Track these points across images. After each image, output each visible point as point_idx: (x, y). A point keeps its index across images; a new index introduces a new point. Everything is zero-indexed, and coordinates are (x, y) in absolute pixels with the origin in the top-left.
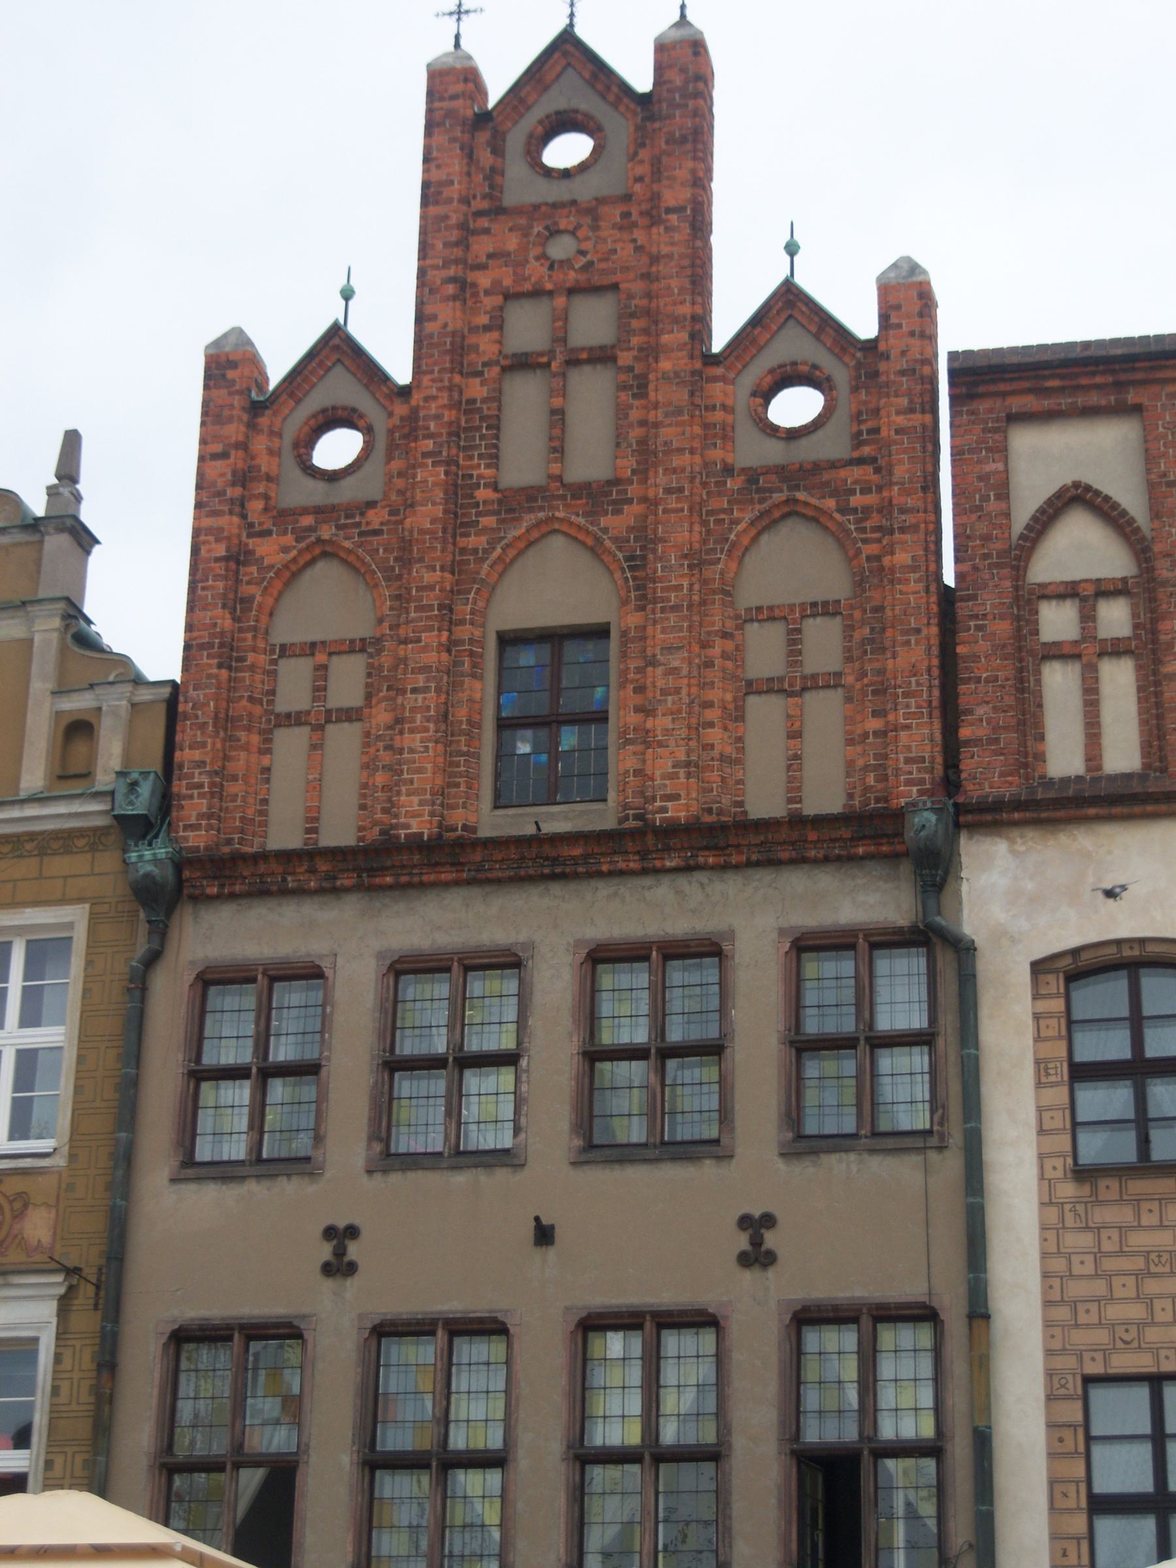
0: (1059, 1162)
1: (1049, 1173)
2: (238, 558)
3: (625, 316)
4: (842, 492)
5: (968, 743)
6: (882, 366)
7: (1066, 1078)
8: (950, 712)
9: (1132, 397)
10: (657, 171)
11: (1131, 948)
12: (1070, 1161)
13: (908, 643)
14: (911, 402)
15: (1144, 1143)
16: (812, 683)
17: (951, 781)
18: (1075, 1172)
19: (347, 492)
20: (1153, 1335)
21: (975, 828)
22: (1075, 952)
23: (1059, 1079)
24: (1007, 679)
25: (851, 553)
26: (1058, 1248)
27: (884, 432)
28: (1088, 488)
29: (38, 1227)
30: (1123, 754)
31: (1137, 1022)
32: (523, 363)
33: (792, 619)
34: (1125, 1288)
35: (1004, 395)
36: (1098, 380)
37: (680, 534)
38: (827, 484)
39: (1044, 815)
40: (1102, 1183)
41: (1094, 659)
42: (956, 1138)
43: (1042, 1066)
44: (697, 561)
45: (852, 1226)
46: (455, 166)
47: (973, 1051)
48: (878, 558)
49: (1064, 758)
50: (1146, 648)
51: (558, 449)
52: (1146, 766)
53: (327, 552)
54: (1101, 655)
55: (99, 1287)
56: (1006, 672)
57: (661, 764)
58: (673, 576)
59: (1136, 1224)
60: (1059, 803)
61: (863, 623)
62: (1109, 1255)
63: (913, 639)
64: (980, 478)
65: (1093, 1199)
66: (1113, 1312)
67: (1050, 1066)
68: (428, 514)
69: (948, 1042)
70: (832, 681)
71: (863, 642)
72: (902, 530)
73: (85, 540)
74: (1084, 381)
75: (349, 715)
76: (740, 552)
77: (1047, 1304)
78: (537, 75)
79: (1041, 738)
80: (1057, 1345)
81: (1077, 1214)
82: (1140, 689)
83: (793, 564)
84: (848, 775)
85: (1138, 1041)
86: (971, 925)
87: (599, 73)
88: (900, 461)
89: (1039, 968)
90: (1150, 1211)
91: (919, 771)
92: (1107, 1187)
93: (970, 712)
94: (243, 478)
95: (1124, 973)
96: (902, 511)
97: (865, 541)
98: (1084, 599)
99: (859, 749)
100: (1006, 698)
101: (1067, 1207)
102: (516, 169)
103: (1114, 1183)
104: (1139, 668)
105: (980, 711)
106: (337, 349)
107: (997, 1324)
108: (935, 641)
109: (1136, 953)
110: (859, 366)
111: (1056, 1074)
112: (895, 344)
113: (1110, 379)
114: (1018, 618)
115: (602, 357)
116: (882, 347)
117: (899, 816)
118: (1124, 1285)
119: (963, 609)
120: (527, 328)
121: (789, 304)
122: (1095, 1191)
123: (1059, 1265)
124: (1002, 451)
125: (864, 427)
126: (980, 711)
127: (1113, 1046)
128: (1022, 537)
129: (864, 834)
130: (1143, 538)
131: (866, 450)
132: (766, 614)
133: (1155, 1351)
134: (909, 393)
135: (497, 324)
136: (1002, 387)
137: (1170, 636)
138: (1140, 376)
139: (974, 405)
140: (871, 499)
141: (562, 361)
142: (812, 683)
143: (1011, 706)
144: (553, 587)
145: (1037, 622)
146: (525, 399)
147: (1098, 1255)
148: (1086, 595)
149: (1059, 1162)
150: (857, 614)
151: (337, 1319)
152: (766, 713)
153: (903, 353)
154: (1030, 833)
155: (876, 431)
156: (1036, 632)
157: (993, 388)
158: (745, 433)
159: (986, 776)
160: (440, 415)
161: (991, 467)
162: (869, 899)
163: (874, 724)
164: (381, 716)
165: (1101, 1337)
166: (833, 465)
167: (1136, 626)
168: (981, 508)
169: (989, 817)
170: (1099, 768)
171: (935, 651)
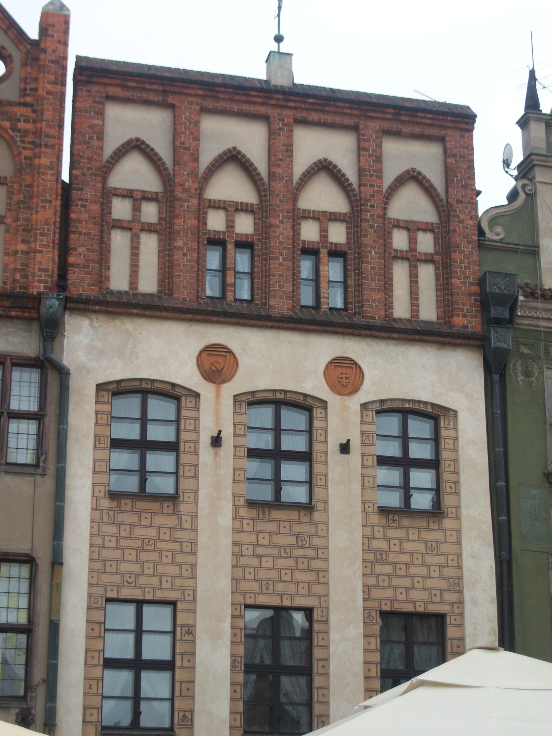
0: (102, 489)
1: (97, 494)
4: (14, 120)
5: (72, 265)
6: (42, 56)
7: (109, 446)
8: (64, 248)
9: (170, 99)
11: (147, 384)
12: (107, 488)
13: (44, 207)
14: (56, 78)
15: (143, 482)
18: (110, 494)
20: (142, 580)
21: (73, 310)
22: (119, 382)
23: (106, 446)
24: (96, 235)
25: (16, 153)
26: (99, 533)
27: (40, 92)
28: (143, 142)
30: (148, 284)
31: (144, 421)
34: (131, 555)
35: (106, 85)
36: (155, 87)
38: (6, 113)
39: (110, 309)
40: (123, 501)
41: (138, 232)
42: (51, 471)
43: (97, 438)
47: (65, 427)
48: (30, 159)
49: (119, 281)
50: (165, 230)
52: (159, 291)
54: (142, 230)
56: (95, 232)
59: (139, 524)
60: (118, 304)
61: (20, 192)
62: (124, 538)
63: (47, 205)
64: (90, 127)
65: (118, 509)
66: (124, 567)
67: (102, 439)
69: (50, 421)
71: (19, 202)
72: (46, 146)
74: (148, 86)
77: (91, 560)
79: (108, 268)
80: (94, 581)
81: (109, 516)
82: (160, 251)
84: (4, 271)
85: (144, 431)
88: (48, 109)
89: (100, 387)
90: (146, 518)
91: (45, 275)
92: (126, 504)
93: (75, 249)
95: (140, 395)
96: (47, 136)
97: (24, 148)
98: (135, 200)
99: (12, 259)
100: (94, 245)
101: (105, 512)
103: (129, 502)
104: (160, 240)
105: (81, 250)
107: (65, 568)
108: (59, 209)
109: (149, 386)
110: (28, 52)
111: (104, 443)
112: (49, 44)
113: (161, 88)
114: (102, 204)
116: (43, 45)
117: (38, 299)
118: (130, 554)
119: (75, 194)
122: (119, 506)
123: (98, 541)
124: (101, 114)
125: (28, 87)
126: (81, 250)
127: (132, 432)
128: (108, 161)
130: (169, 174)
131: (28, 99)
133: (143, 588)
134: (55, 73)
136: (106, 81)
137: (179, 227)
138: (176, 89)
139: (90, 87)
140: (29, 126)
143: (96, 250)
145: (111, 207)
147: (118, 538)
149: (102, 489)
150: (16, 186)
153: (54, 51)
154: (102, 317)
155: (35, 90)
156: (110, 213)
157: (101, 80)
159: (80, 284)
161: (96, 122)
163: (21, 247)
165: (117, 579)
166: (10, 104)
167: (160, 219)
168: (88, 143)
169: (82, 306)
170: (136, 289)
171: (59, 214)
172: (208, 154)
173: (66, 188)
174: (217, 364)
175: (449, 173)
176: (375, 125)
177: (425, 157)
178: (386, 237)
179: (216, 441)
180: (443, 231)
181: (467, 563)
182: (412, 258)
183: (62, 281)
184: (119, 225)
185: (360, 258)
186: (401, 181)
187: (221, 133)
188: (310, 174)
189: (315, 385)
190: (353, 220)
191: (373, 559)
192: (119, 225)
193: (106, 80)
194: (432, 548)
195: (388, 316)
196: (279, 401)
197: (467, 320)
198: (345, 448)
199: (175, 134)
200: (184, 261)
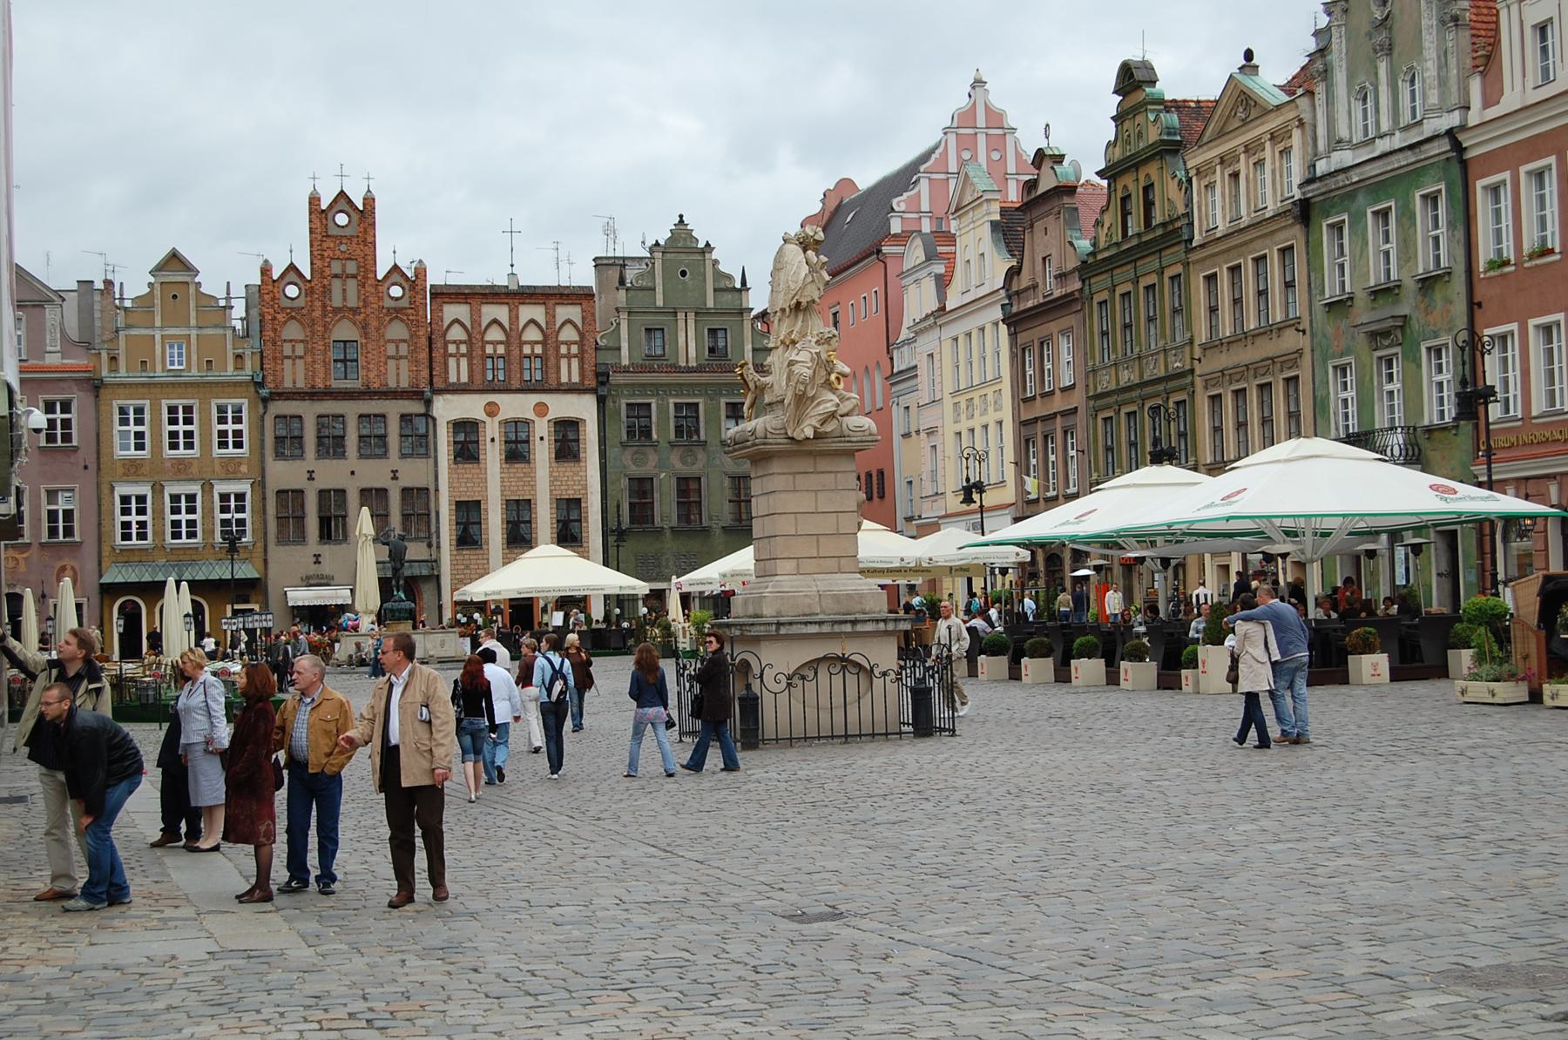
2: (274, 319)
8: (431, 369)
17: (431, 383)
29: (244, 469)
30: (464, 378)
32: (336, 276)
33: (397, 342)
37: (374, 323)
44: (378, 329)
45: (414, 473)
49: (453, 379)
50: (469, 356)
51: (345, 299)
55: (260, 485)
57: (372, 375)
68: (317, 314)
78: (335, 200)
83: (397, 330)
86: (435, 414)
87: (350, 202)
102: (331, 224)
115: (354, 276)
120: (336, 267)
121: (396, 267)
129: (414, 394)
144: (345, 330)
146: (337, 283)
148: (457, 343)
152: (391, 363)
158: (386, 299)
159: (438, 383)
174: (492, 410)
177: (574, 312)
178: (557, 349)
180: (581, 344)
186: (563, 324)
187: (491, 311)
188: (525, 326)
189: (530, 415)
190: (544, 343)
193: (445, 294)
194: (576, 474)
195: (559, 384)
196: (516, 422)
197: (591, 382)
200: (477, 369)
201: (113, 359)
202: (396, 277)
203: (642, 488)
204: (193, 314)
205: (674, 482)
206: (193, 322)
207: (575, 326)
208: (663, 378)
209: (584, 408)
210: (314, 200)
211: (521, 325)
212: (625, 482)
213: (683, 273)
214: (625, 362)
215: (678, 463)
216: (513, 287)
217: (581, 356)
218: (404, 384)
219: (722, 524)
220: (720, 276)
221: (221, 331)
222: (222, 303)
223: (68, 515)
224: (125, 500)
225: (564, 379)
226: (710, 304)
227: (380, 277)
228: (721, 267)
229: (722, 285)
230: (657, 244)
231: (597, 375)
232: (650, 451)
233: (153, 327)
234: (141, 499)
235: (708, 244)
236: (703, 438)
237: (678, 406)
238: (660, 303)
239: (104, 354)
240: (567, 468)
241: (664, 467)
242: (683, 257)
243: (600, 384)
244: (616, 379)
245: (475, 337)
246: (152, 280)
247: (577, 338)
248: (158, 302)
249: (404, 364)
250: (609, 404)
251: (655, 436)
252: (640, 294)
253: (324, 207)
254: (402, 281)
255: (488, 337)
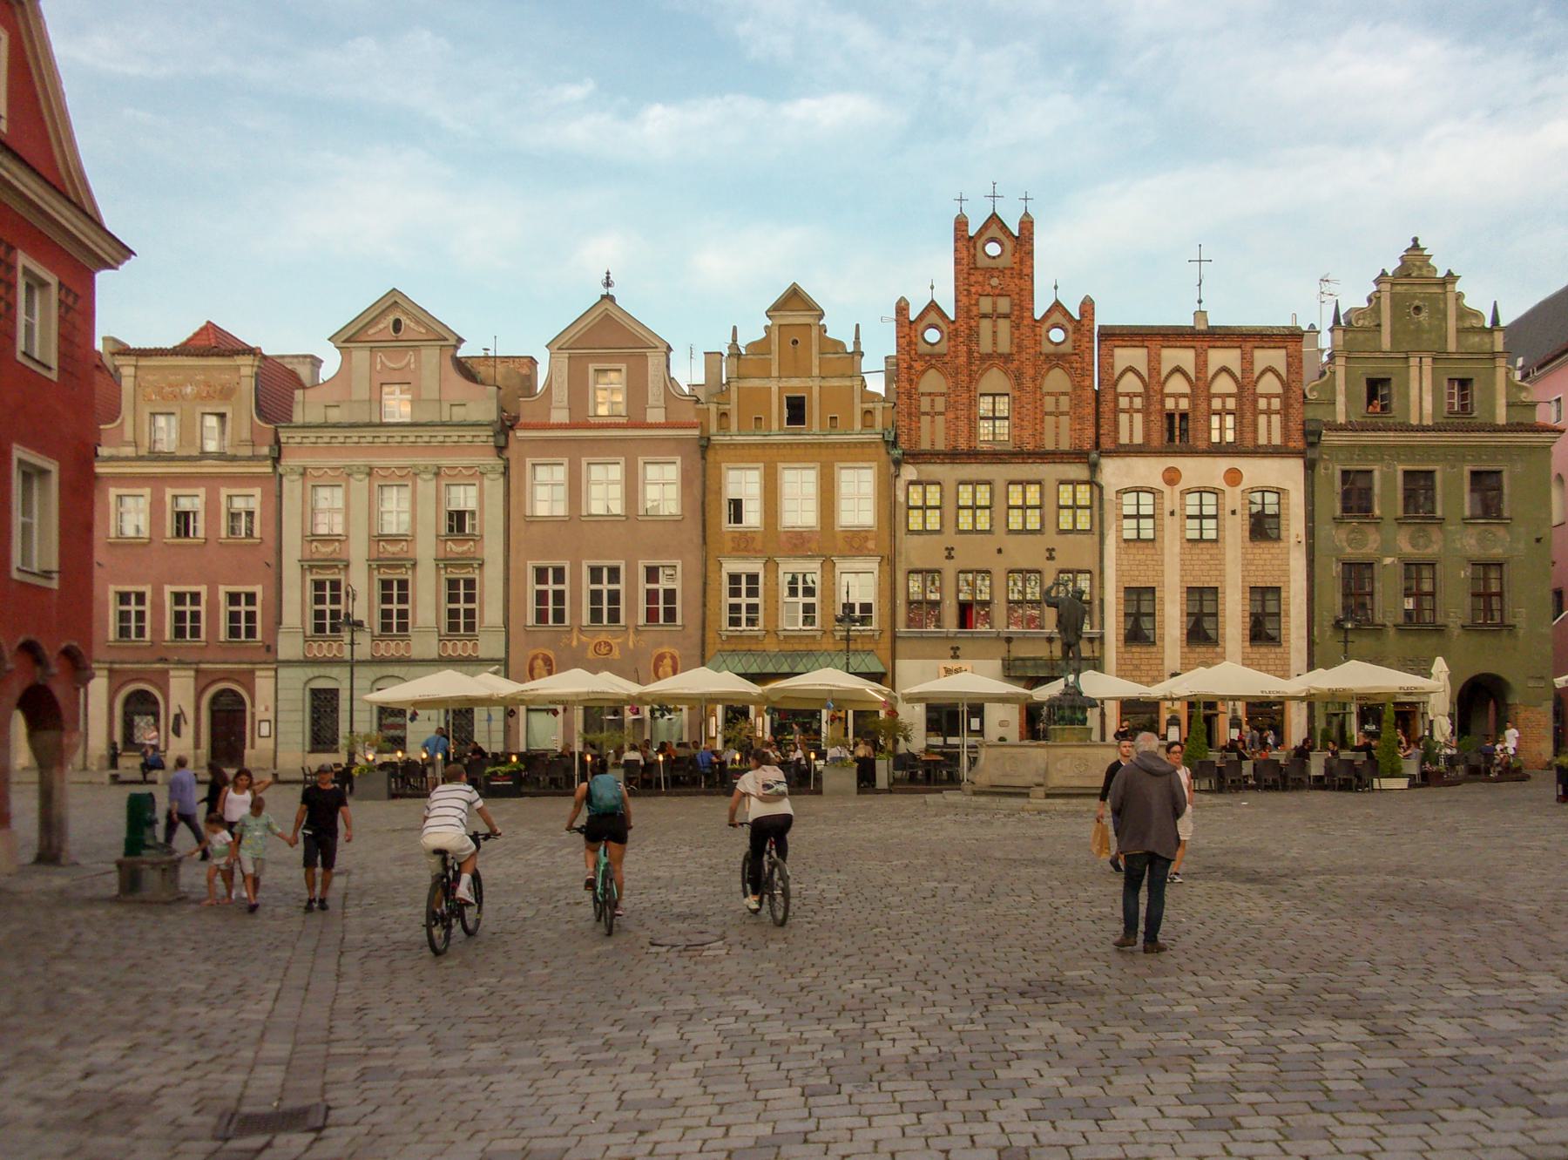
2: (910, 367)
3: (1012, 305)
8: (1098, 426)
10: (1021, 262)
16: (1062, 414)
19: (937, 349)
29: (871, 545)
32: (985, 316)
42: (1097, 532)
44: (1034, 380)
46: (965, 254)
50: (1146, 412)
51: (995, 343)
53: (932, 366)
58: (1028, 384)
68: (962, 360)
69: (1096, 508)
70: (1067, 414)
73: (862, 355)
75: (941, 414)
76: (1043, 377)
78: (985, 226)
83: (1057, 380)
87: (1003, 227)
94: (910, 343)
102: (980, 254)
106: (933, 306)
112: (1085, 322)
115: (1006, 316)
120: (986, 305)
121: (1057, 305)
132: (1050, 394)
135: (977, 304)
141: (994, 316)
142: (1062, 414)
146: (986, 325)
151: (949, 568)
158: (1045, 343)
159: (1106, 443)
160: (963, 328)
162: (1079, 471)
164: (951, 415)
172: (1165, 369)
173: (1097, 393)
174: (1172, 477)
175: (1289, 365)
176: (1250, 345)
178: (1255, 402)
179: (1172, 513)
181: (1292, 563)
182: (1269, 412)
183: (1097, 445)
184: (1123, 411)
185: (1242, 417)
186: (1263, 373)
189: (1220, 483)
191: (1247, 563)
192: (1123, 411)
193: (1113, 336)
197: (1297, 443)
198: (1234, 512)
199: (1149, 361)
201: (724, 415)
202: (1057, 317)
203: (1357, 574)
204: (816, 362)
205: (1401, 570)
206: (816, 371)
207: (1278, 376)
208: (1390, 437)
209: (1287, 474)
210: (961, 224)
211: (1211, 373)
212: (1336, 569)
213: (1418, 309)
214: (1341, 419)
215: (1404, 543)
216: (1201, 327)
217: (1285, 412)
218: (1065, 445)
219: (1460, 622)
220: (1464, 313)
221: (847, 383)
222: (850, 349)
223: (670, 595)
224: (735, 579)
225: (1262, 440)
226: (1452, 346)
227: (1038, 315)
228: (1467, 302)
229: (1467, 325)
230: (1384, 274)
231: (1306, 434)
232: (1371, 530)
233: (769, 377)
234: (753, 578)
235: (1449, 274)
236: (1439, 513)
237: (1406, 473)
238: (1386, 343)
239: (713, 408)
240: (1264, 550)
241: (1388, 545)
242: (1417, 289)
243: (1307, 443)
244: (1329, 438)
245: (1153, 388)
246: (769, 323)
247: (1280, 390)
248: (775, 348)
249: (1065, 420)
250: (1320, 470)
251: (1377, 512)
252: (1361, 336)
253: (972, 233)
254: (1063, 321)
255: (1169, 389)
